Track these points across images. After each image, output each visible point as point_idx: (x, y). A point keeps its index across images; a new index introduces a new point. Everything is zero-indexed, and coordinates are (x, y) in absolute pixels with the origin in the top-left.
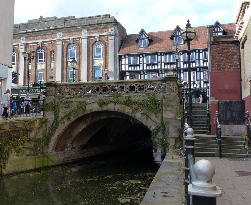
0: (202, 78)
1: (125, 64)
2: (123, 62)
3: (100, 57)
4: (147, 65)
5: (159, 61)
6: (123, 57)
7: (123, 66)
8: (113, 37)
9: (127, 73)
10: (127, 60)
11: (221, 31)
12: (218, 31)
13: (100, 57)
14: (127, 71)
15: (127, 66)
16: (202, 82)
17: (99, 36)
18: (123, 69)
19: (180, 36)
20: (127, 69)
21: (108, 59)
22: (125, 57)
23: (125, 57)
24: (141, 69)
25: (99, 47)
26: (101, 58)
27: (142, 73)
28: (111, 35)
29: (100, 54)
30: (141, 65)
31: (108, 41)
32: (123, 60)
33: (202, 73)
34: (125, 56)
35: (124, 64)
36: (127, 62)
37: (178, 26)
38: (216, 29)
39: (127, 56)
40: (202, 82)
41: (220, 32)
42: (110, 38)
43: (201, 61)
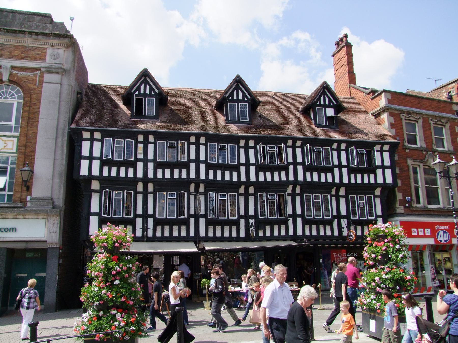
0: (299, 212)
1: (91, 158)
2: (85, 151)
3: (9, 129)
4: (158, 165)
5: (193, 156)
6: (86, 135)
7: (84, 164)
8: (55, 77)
9: (95, 185)
10: (97, 145)
11: (331, 105)
12: (327, 103)
13: (9, 129)
14: (95, 178)
15: (96, 164)
16: (299, 220)
17: (13, 67)
18: (84, 171)
19: (241, 101)
20: (96, 172)
21: (36, 137)
22: (92, 135)
23: (92, 135)
24: (140, 175)
25: (9, 101)
26: (13, 133)
27: (140, 187)
28: (50, 71)
29: (10, 121)
30: (140, 165)
31: (41, 85)
32: (86, 145)
33: (298, 199)
34: (92, 132)
35: (85, 158)
36: (96, 153)
37: (238, 77)
38: (322, 98)
39: (97, 135)
40: (299, 220)
41: (329, 106)
42: (47, 77)
43: (300, 169)
